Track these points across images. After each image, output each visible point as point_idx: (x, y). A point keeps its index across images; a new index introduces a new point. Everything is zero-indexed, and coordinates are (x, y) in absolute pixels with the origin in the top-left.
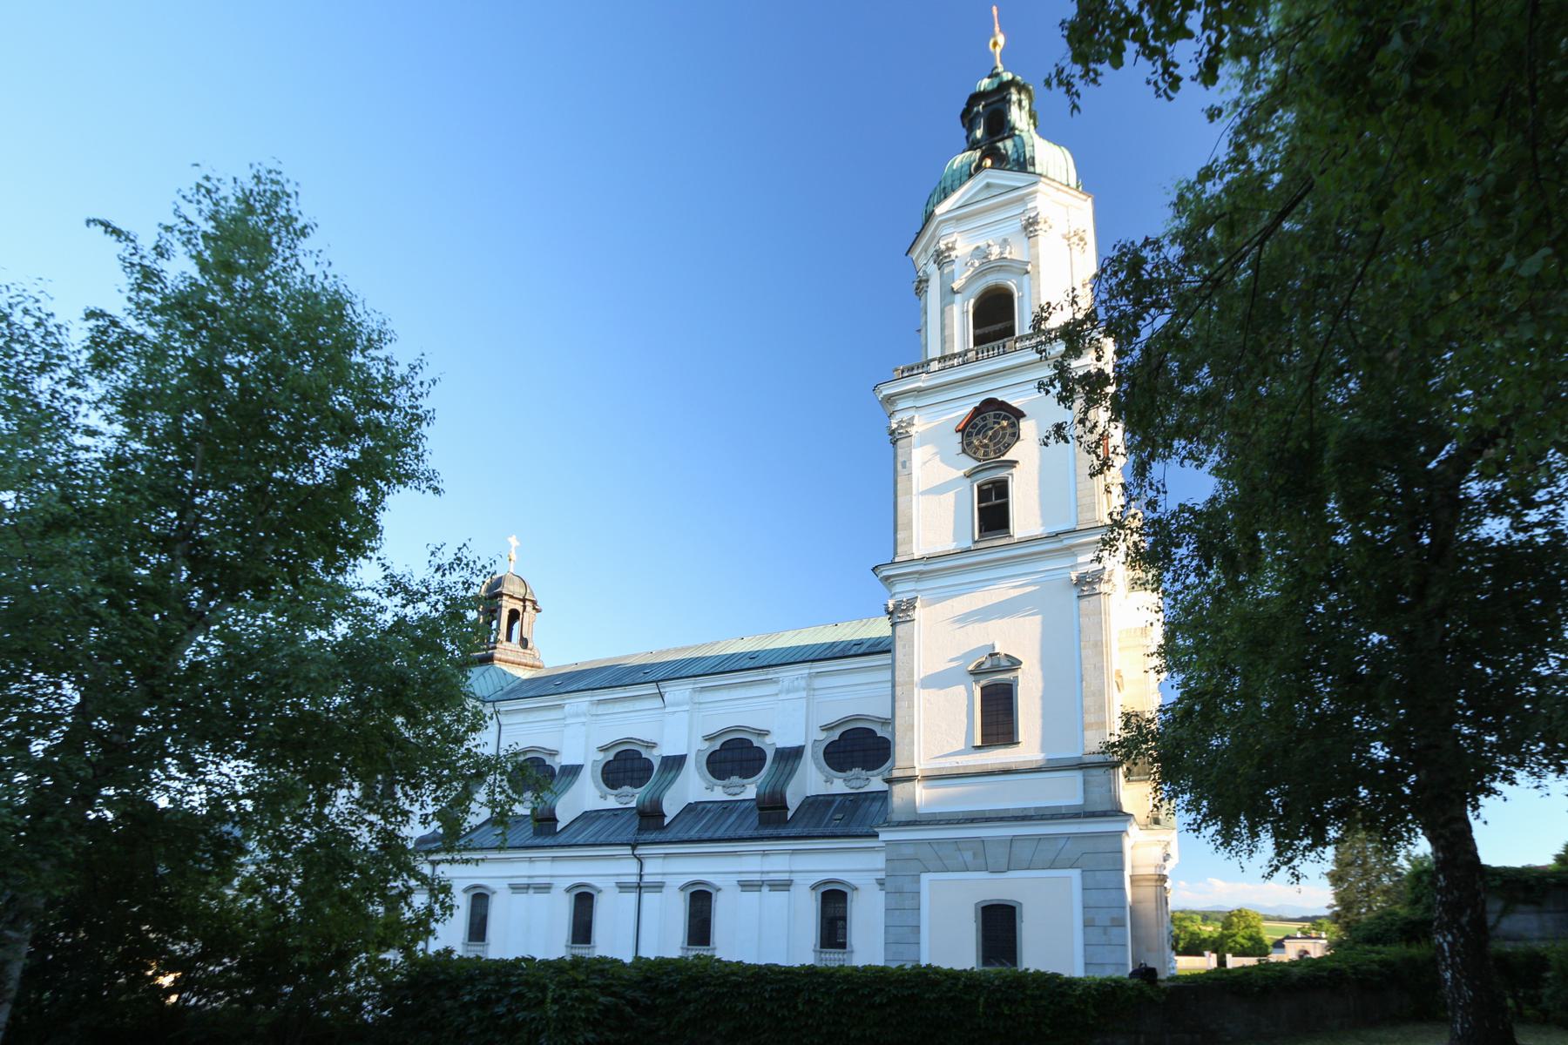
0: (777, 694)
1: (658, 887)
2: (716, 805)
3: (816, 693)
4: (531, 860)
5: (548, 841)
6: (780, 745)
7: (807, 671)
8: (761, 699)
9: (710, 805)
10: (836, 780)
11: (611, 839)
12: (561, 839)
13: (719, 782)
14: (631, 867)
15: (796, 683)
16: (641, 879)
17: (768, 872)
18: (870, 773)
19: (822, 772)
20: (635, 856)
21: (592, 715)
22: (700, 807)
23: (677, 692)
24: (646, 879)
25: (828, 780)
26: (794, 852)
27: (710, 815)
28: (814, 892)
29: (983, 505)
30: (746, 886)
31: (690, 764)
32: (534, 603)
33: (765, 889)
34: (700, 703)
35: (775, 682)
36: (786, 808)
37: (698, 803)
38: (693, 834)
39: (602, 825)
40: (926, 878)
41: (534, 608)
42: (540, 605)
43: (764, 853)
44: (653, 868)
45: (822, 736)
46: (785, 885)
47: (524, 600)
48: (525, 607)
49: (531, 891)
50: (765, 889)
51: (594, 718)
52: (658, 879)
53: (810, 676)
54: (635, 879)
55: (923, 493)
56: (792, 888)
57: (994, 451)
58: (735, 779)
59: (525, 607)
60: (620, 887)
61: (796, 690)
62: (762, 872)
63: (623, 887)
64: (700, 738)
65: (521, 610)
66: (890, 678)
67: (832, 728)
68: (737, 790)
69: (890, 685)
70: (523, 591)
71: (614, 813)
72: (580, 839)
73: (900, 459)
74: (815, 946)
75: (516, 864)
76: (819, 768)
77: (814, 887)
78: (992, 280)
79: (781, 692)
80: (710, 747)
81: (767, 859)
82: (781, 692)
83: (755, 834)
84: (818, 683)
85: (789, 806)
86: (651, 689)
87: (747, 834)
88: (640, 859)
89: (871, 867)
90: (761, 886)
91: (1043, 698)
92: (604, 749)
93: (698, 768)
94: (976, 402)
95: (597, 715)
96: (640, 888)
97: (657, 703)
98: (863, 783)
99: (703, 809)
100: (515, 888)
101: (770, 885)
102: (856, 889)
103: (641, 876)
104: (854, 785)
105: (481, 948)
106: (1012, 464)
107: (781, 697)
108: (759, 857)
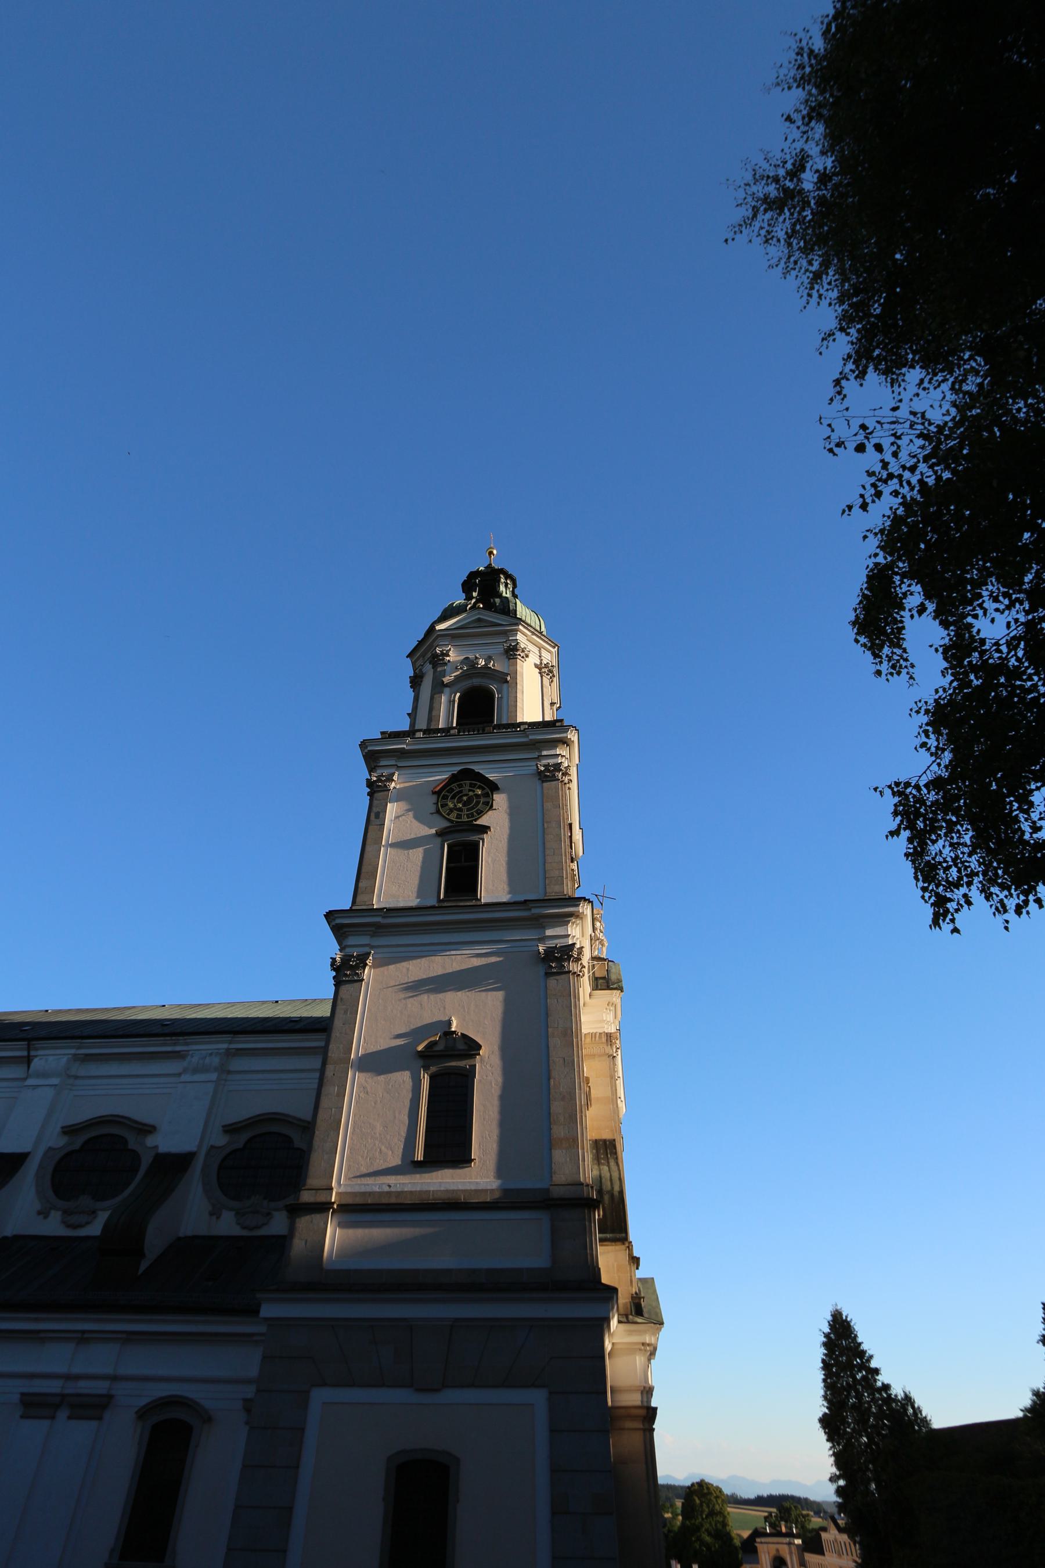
0: (180, 1075)
6: (163, 1149)
7: (225, 1046)
17: (78, 1377)
29: (452, 865)
33: (63, 1414)
36: (142, 1255)
40: (319, 1396)
55: (393, 845)
57: (467, 815)
62: (68, 1377)
64: (58, 1129)
73: (375, 810)
78: (476, 682)
79: (185, 1071)
82: (185, 1071)
91: (502, 1098)
94: (456, 769)
106: (485, 829)
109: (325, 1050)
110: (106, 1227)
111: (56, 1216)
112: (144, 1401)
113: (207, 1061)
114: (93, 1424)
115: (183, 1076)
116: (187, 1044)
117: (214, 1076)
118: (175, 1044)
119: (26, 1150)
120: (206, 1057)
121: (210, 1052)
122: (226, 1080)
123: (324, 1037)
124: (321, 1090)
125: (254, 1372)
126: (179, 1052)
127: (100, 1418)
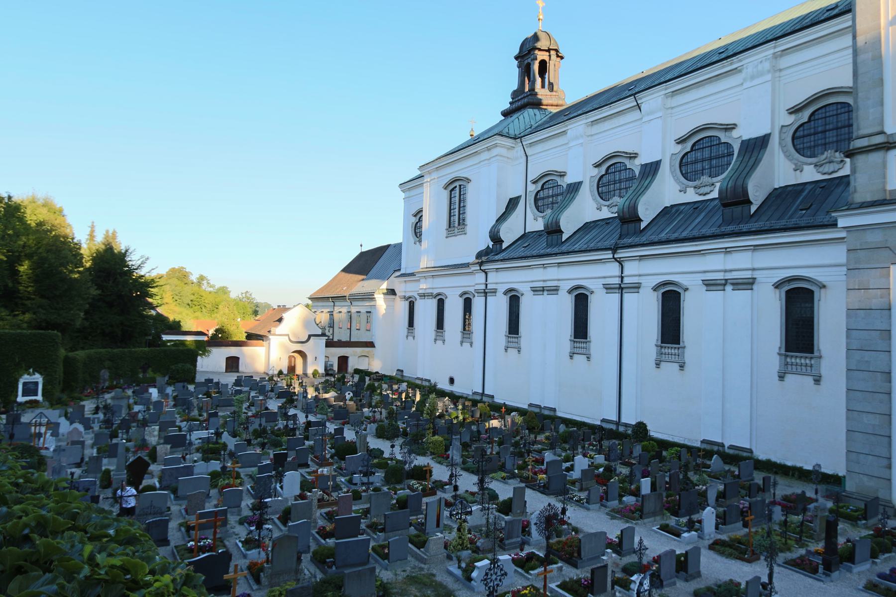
0: (742, 84)
1: (636, 287)
2: (688, 207)
4: (544, 266)
5: (556, 250)
7: (772, 51)
10: (806, 167)
11: (600, 245)
12: (564, 248)
13: (691, 183)
14: (613, 269)
15: (760, 67)
16: (622, 281)
17: (731, 271)
19: (790, 160)
20: (616, 259)
21: (588, 136)
22: (674, 210)
23: (652, 100)
24: (626, 280)
25: (798, 169)
26: (756, 248)
28: (777, 291)
30: (710, 285)
31: (665, 169)
32: (557, 51)
33: (729, 288)
34: (672, 108)
37: (672, 206)
38: (663, 236)
39: (599, 230)
41: (558, 56)
42: (562, 52)
43: (727, 251)
44: (631, 268)
45: (790, 119)
46: (748, 284)
47: (549, 50)
48: (550, 56)
50: (729, 288)
51: (590, 138)
52: (635, 280)
53: (776, 56)
54: (617, 281)
56: (755, 287)
59: (550, 56)
61: (761, 74)
62: (725, 271)
63: (608, 288)
65: (547, 59)
66: (850, 43)
68: (707, 189)
69: (850, 51)
70: (548, 43)
71: (607, 221)
72: (577, 247)
74: (780, 348)
75: (535, 270)
76: (788, 156)
77: (777, 286)
79: (745, 80)
80: (683, 149)
81: (729, 257)
82: (745, 80)
83: (718, 231)
84: (785, 62)
85: (751, 198)
86: (630, 102)
87: (709, 233)
88: (620, 262)
90: (725, 285)
95: (592, 135)
96: (622, 289)
97: (636, 114)
98: (837, 166)
99: (677, 211)
101: (733, 284)
102: (824, 286)
103: (622, 278)
105: (515, 340)
107: (745, 86)
109: (853, 27)
110: (720, 192)
111: (691, 191)
112: (776, 280)
113: (760, 67)
114: (748, 293)
115: (744, 84)
116: (740, 61)
117: (769, 77)
118: (731, 64)
119: (658, 159)
120: (758, 65)
121: (760, 60)
122: (780, 77)
123: (851, 16)
124: (856, 60)
125: (843, 260)
126: (736, 68)
127: (752, 289)
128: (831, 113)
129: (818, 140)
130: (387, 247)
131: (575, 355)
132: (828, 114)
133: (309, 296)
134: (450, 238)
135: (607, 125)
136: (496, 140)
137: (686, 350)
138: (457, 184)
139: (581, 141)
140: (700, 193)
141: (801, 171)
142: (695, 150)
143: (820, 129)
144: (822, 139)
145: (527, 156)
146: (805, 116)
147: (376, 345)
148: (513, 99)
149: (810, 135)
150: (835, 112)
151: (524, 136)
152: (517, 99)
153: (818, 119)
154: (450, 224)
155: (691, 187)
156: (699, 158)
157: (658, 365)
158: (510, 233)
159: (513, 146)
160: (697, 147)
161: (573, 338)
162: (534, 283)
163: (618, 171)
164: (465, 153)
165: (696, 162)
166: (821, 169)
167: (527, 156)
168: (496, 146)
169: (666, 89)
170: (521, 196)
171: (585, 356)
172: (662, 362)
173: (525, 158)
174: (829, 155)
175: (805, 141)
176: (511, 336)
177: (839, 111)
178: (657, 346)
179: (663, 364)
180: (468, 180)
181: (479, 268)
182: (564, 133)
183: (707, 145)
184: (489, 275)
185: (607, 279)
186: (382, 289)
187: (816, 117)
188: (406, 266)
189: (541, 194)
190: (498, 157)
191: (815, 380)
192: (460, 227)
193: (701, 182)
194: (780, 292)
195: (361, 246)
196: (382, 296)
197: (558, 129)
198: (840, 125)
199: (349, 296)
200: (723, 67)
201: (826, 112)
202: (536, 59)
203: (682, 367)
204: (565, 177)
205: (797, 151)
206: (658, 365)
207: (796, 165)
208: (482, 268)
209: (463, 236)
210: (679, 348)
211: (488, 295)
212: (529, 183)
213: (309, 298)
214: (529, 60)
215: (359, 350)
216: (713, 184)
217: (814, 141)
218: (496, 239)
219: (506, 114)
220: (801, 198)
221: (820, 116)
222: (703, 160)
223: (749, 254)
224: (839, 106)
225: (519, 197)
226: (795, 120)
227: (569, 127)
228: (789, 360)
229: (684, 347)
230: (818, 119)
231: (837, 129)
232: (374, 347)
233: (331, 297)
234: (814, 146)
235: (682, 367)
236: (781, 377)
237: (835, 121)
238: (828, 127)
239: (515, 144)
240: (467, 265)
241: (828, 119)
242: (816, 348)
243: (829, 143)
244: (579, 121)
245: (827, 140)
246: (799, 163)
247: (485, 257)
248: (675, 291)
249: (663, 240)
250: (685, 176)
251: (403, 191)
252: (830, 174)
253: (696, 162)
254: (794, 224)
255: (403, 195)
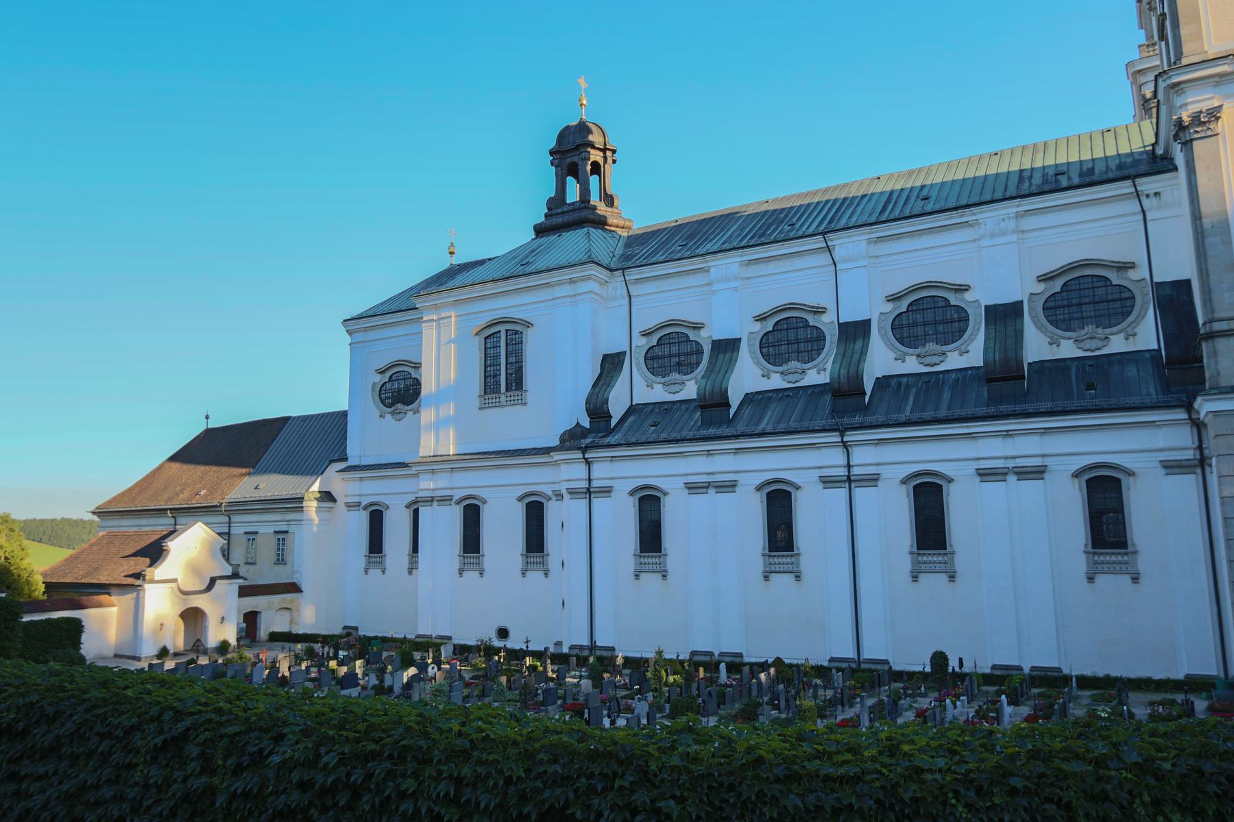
1: (873, 480)
3: (1026, 235)
4: (709, 453)
7: (1015, 210)
8: (952, 248)
9: (905, 380)
13: (911, 351)
15: (1003, 225)
17: (1014, 457)
18: (1108, 331)
24: (855, 471)
25: (1054, 342)
26: (1047, 431)
27: (913, 391)
28: (1076, 480)
30: (985, 475)
33: (1012, 479)
35: (972, 226)
43: (1008, 434)
44: (865, 457)
45: (1040, 287)
47: (604, 150)
48: (605, 158)
49: (712, 491)
50: (1012, 479)
53: (1018, 216)
54: (842, 472)
56: (1046, 476)
58: (931, 347)
59: (605, 158)
60: (824, 482)
61: (1004, 233)
62: (1006, 458)
63: (828, 482)
65: (601, 162)
67: (1052, 278)
68: (935, 359)
70: (602, 140)
74: (1086, 545)
75: (690, 460)
80: (895, 309)
81: (1009, 441)
84: (1029, 223)
89: (1147, 447)
92: (761, 318)
93: (883, 336)
97: (824, 258)
98: (1100, 343)
100: (692, 488)
101: (1017, 473)
102: (1133, 474)
104: (1088, 346)
107: (984, 243)
108: (1000, 439)
116: (974, 214)
118: (961, 216)
128: (1086, 286)
129: (1074, 313)
130: (286, 420)
131: (772, 575)
132: (1082, 287)
133: (92, 509)
134: (488, 411)
135: (772, 267)
136: (592, 270)
137: (956, 556)
138: (502, 328)
139: (734, 284)
140: (926, 363)
141: (1058, 346)
142: (912, 311)
143: (1074, 301)
144: (1077, 312)
145: (630, 296)
146: (1057, 285)
147: (303, 589)
148: (549, 209)
149: (1063, 307)
150: (1090, 285)
151: (629, 268)
152: (559, 211)
153: (1071, 291)
154: (490, 386)
155: (912, 355)
156: (918, 321)
157: (799, 577)
158: (617, 405)
159: (607, 279)
160: (914, 308)
161: (767, 552)
162: (690, 477)
163: (794, 328)
164: (522, 283)
165: (915, 324)
166: (1082, 345)
167: (630, 296)
168: (588, 278)
169: (870, 233)
170: (625, 352)
171: (792, 575)
172: (921, 575)
173: (627, 299)
174: (1090, 331)
175: (1058, 313)
176: (531, 554)
177: (1095, 285)
178: (911, 553)
179: (922, 577)
180: (528, 325)
181: (581, 456)
182: (707, 270)
183: (929, 307)
184: (595, 467)
185: (824, 470)
186: (313, 492)
187: (1069, 288)
188: (356, 450)
189: (658, 352)
190: (591, 295)
191: (1133, 579)
192: (508, 394)
193: (925, 350)
194: (1080, 481)
195: (207, 417)
196: (315, 504)
197: (689, 265)
198: (1097, 299)
199: (226, 506)
200: (951, 218)
201: (1079, 284)
202: (589, 160)
203: (952, 577)
204: (702, 330)
205: (1051, 322)
206: (915, 578)
207: (1051, 338)
208: (586, 456)
209: (518, 407)
210: (945, 554)
211: (592, 496)
212: (635, 333)
213: (94, 513)
214: (575, 159)
215: (276, 599)
216: (944, 354)
217: (1069, 313)
218: (597, 410)
219: (540, 231)
220: (1073, 376)
221: (1073, 287)
222: (925, 324)
223: (1037, 438)
224: (1095, 279)
225: (625, 352)
226: (1045, 289)
227: (710, 264)
228: (642, 560)
229: (953, 553)
230: (1071, 291)
231: (1095, 303)
232: (301, 591)
233: (171, 509)
234: (1070, 320)
235: (952, 577)
236: (1091, 579)
237: (1091, 294)
238: (1083, 300)
239: (610, 278)
240: (547, 451)
241: (1082, 291)
242: (1129, 544)
243: (1087, 317)
244: (732, 257)
245: (1084, 314)
246: (1055, 337)
247: (573, 440)
248: (932, 483)
249: (914, 420)
250: (901, 340)
251: (350, 333)
252: (1093, 351)
253: (915, 324)
254: (1093, 405)
255: (348, 339)
